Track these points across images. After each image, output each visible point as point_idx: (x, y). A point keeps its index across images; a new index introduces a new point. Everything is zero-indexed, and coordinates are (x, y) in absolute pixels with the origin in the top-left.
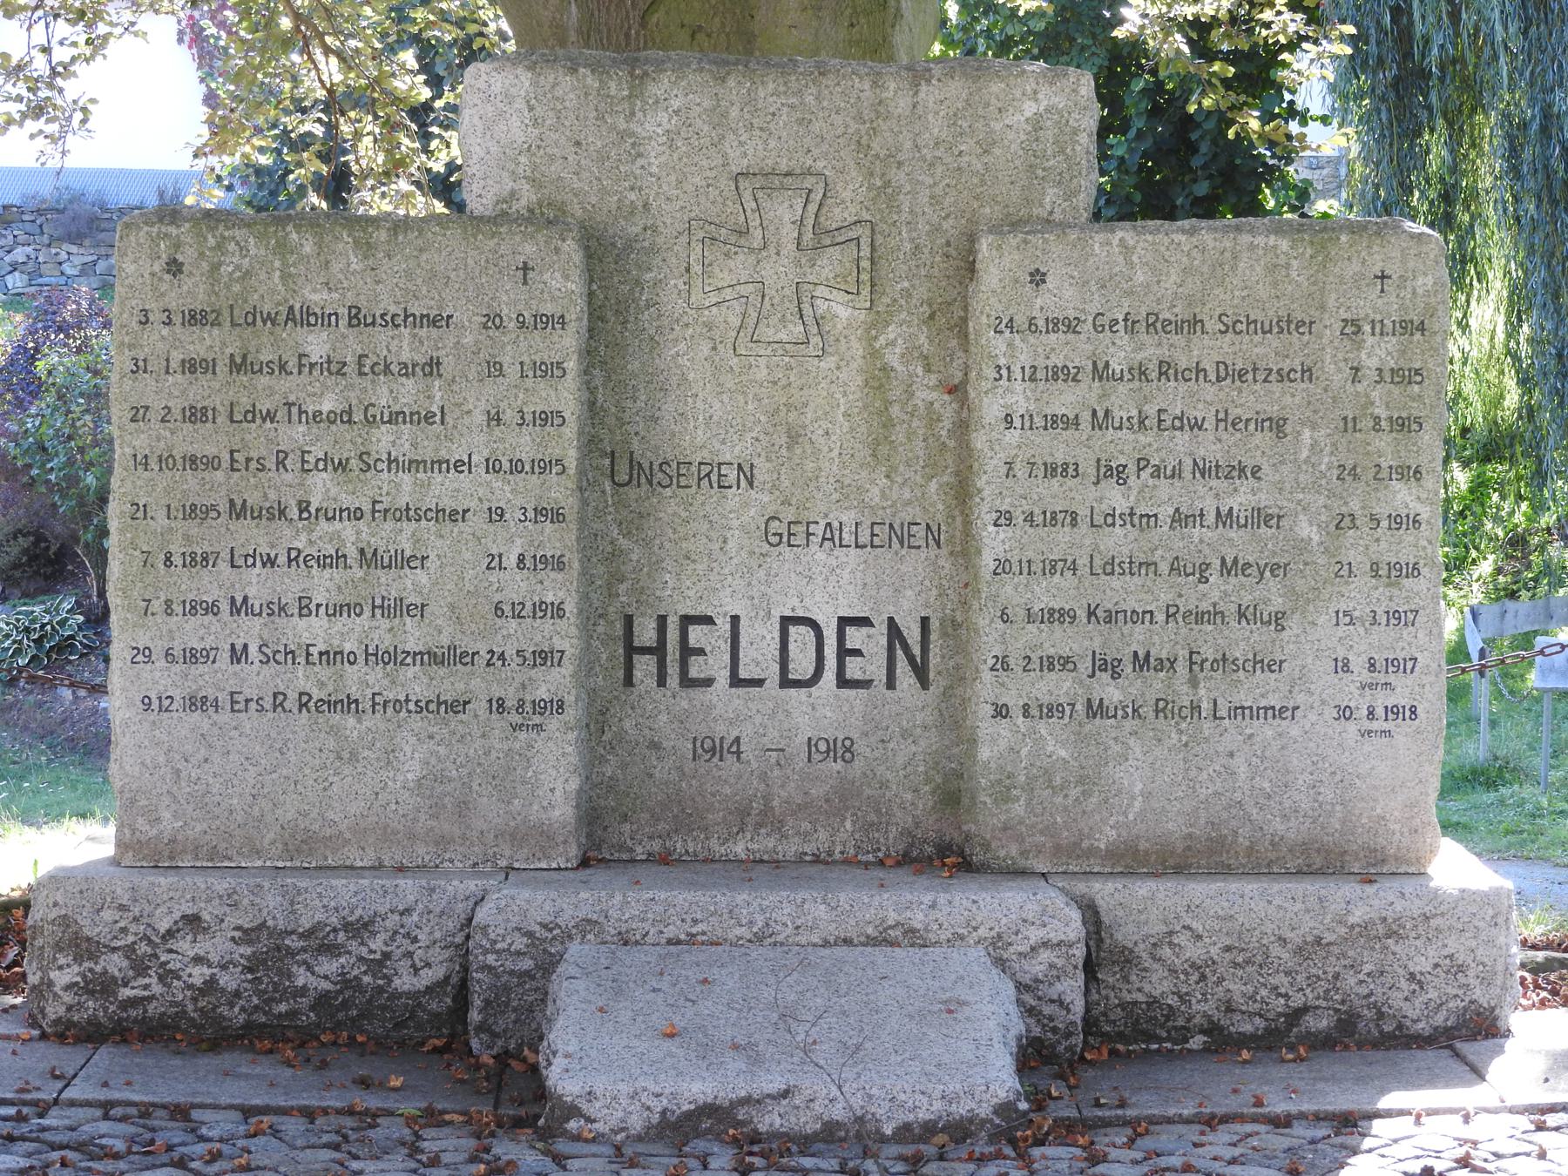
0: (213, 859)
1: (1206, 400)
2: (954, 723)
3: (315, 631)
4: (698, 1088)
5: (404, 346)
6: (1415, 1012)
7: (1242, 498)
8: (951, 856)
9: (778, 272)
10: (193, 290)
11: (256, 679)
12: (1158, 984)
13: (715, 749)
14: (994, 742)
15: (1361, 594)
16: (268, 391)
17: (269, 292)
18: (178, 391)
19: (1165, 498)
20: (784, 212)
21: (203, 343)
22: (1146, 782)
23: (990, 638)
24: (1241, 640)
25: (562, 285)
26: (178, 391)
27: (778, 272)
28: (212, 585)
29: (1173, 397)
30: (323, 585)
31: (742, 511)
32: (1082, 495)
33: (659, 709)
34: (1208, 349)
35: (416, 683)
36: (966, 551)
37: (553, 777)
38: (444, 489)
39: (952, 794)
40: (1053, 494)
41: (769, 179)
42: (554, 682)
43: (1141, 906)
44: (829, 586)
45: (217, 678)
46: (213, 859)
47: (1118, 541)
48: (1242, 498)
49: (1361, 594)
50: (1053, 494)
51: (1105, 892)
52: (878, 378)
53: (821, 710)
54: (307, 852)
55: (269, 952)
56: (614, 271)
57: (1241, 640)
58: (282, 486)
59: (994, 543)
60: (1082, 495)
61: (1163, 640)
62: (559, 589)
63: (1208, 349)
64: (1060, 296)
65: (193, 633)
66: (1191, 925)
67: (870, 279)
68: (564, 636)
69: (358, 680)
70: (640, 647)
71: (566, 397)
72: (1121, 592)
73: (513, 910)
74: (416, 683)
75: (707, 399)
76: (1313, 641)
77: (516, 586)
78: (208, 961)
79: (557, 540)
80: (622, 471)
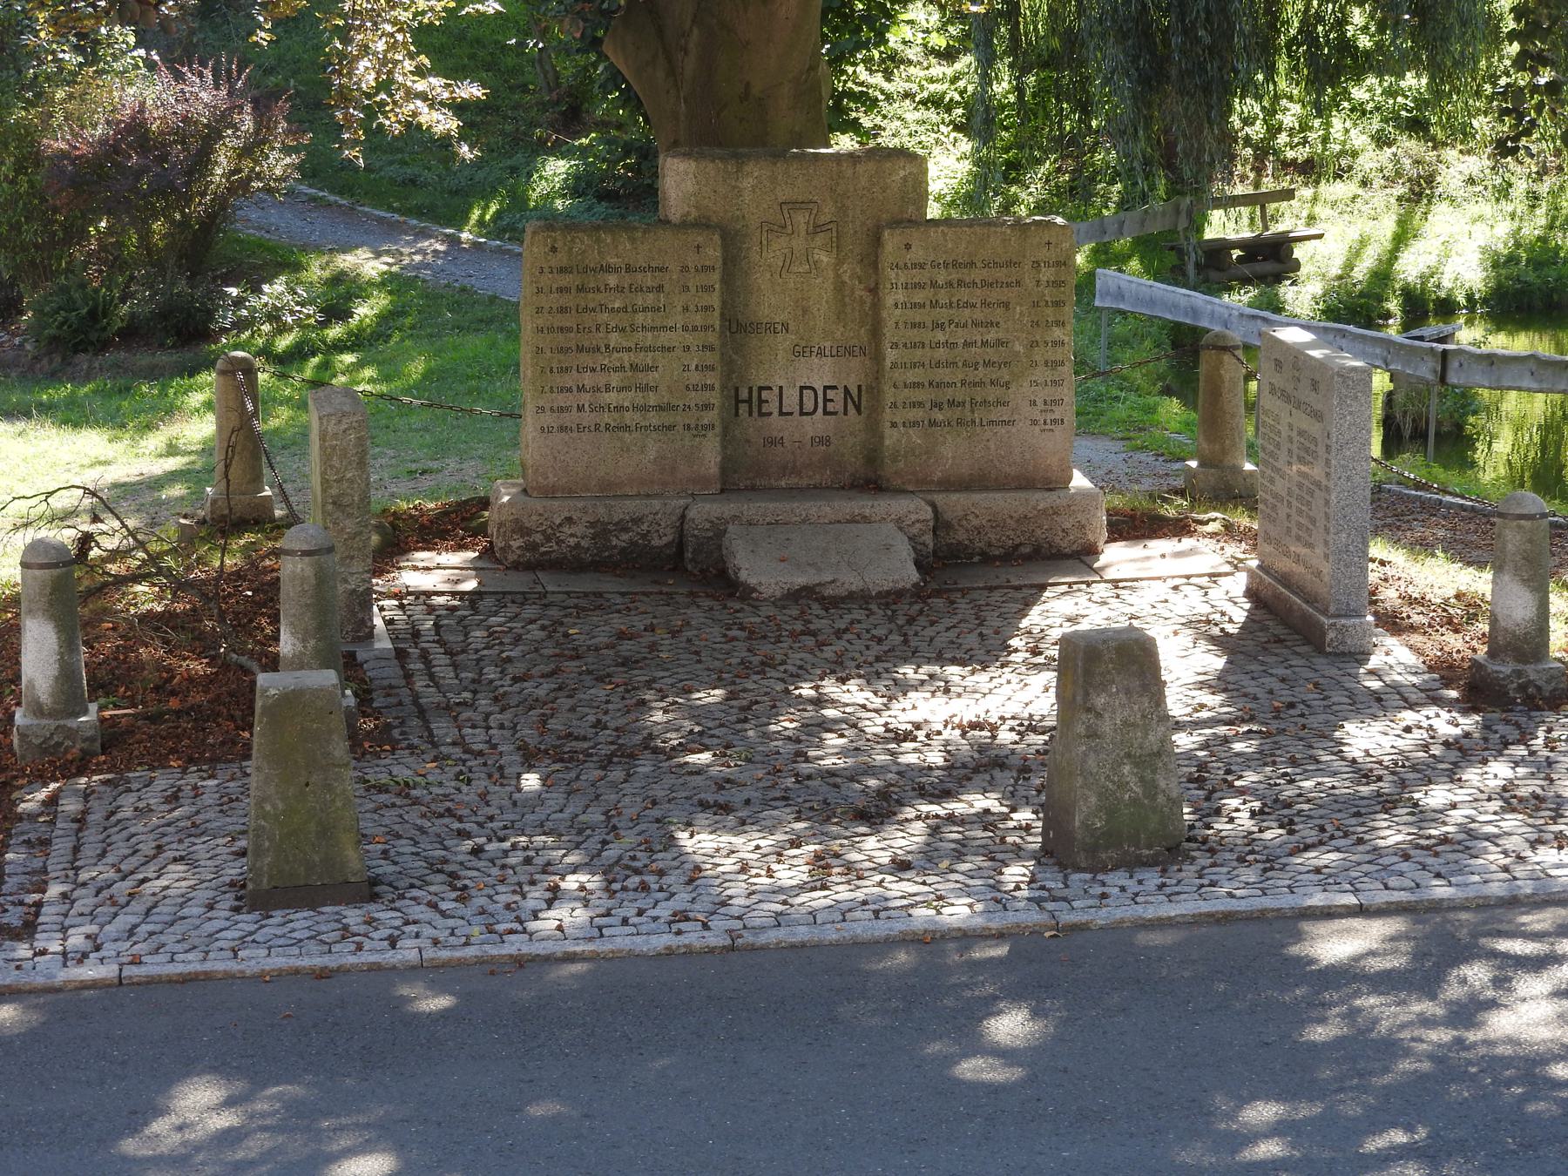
0: (570, 493)
1: (977, 295)
2: (873, 428)
3: (612, 398)
4: (801, 580)
5: (649, 280)
6: (1064, 545)
7: (992, 335)
8: (872, 483)
9: (798, 243)
10: (561, 259)
11: (588, 418)
12: (961, 536)
13: (773, 442)
14: (891, 438)
15: (1041, 374)
16: (593, 299)
17: (593, 258)
18: (555, 300)
19: (961, 336)
20: (801, 219)
21: (566, 279)
22: (953, 452)
23: (889, 395)
24: (992, 393)
25: (714, 253)
26: (555, 300)
27: (798, 243)
28: (569, 380)
29: (964, 294)
30: (615, 379)
31: (784, 342)
32: (927, 336)
33: (750, 426)
34: (977, 275)
35: (654, 419)
36: (878, 357)
37: (710, 455)
38: (665, 338)
39: (873, 456)
40: (914, 335)
41: (794, 205)
42: (710, 417)
43: (954, 504)
44: (819, 373)
45: (571, 418)
46: (570, 493)
47: (941, 353)
48: (992, 335)
49: (1041, 374)
50: (914, 335)
51: (939, 499)
52: (840, 286)
53: (817, 425)
54: (608, 490)
55: (601, 531)
56: (732, 241)
57: (992, 393)
58: (598, 338)
59: (891, 355)
60: (927, 336)
61: (960, 394)
62: (712, 379)
63: (977, 275)
64: (917, 254)
65: (561, 400)
66: (977, 510)
67: (837, 245)
68: (715, 398)
69: (630, 418)
70: (743, 400)
71: (715, 300)
72: (944, 374)
73: (704, 512)
74: (654, 419)
75: (770, 299)
76: (1022, 392)
77: (695, 378)
78: (576, 536)
79: (711, 358)
80: (737, 328)
